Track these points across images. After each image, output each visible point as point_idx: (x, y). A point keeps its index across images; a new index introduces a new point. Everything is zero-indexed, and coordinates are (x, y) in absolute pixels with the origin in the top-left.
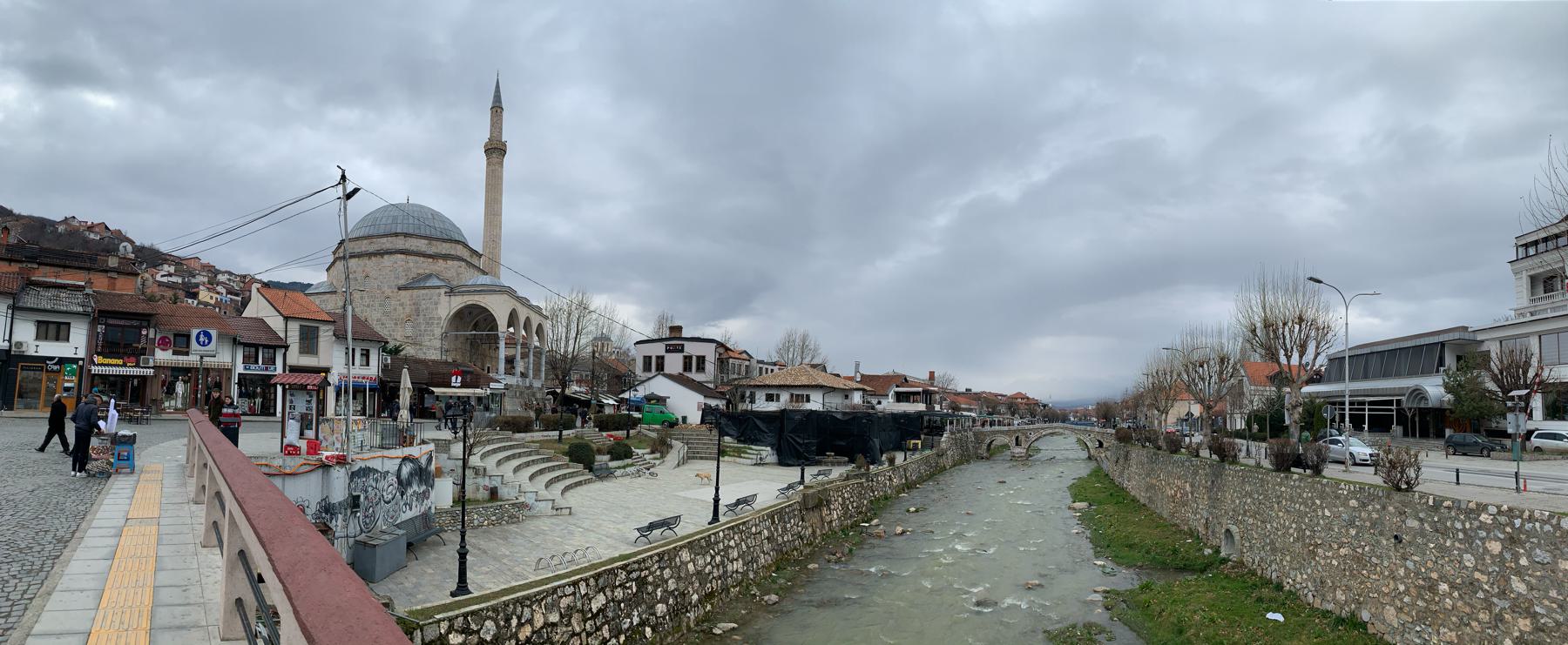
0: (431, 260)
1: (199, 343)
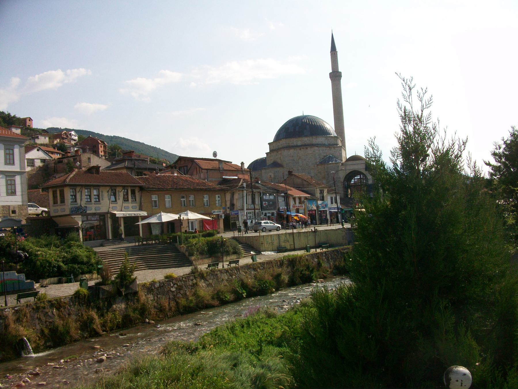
0: (328, 148)
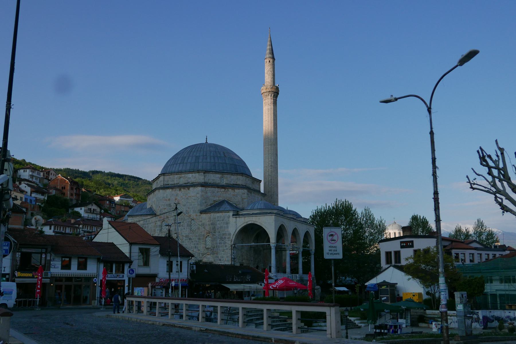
0: (223, 190)
1: (130, 273)
